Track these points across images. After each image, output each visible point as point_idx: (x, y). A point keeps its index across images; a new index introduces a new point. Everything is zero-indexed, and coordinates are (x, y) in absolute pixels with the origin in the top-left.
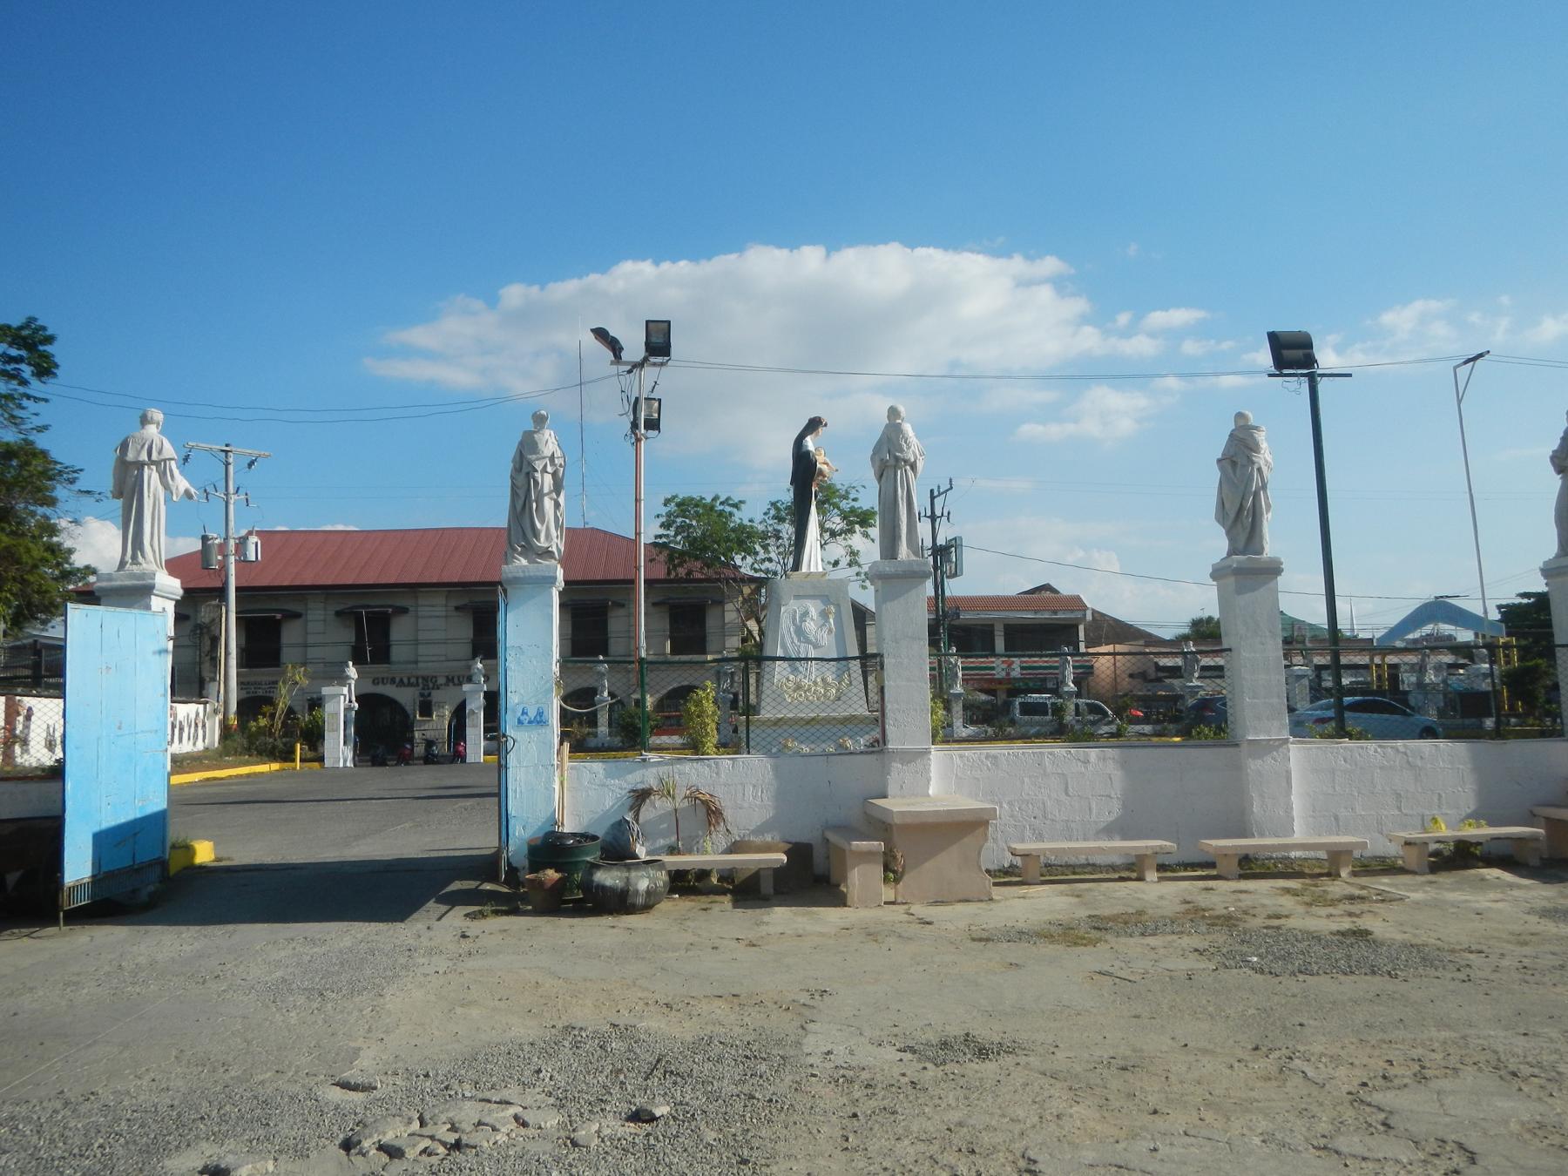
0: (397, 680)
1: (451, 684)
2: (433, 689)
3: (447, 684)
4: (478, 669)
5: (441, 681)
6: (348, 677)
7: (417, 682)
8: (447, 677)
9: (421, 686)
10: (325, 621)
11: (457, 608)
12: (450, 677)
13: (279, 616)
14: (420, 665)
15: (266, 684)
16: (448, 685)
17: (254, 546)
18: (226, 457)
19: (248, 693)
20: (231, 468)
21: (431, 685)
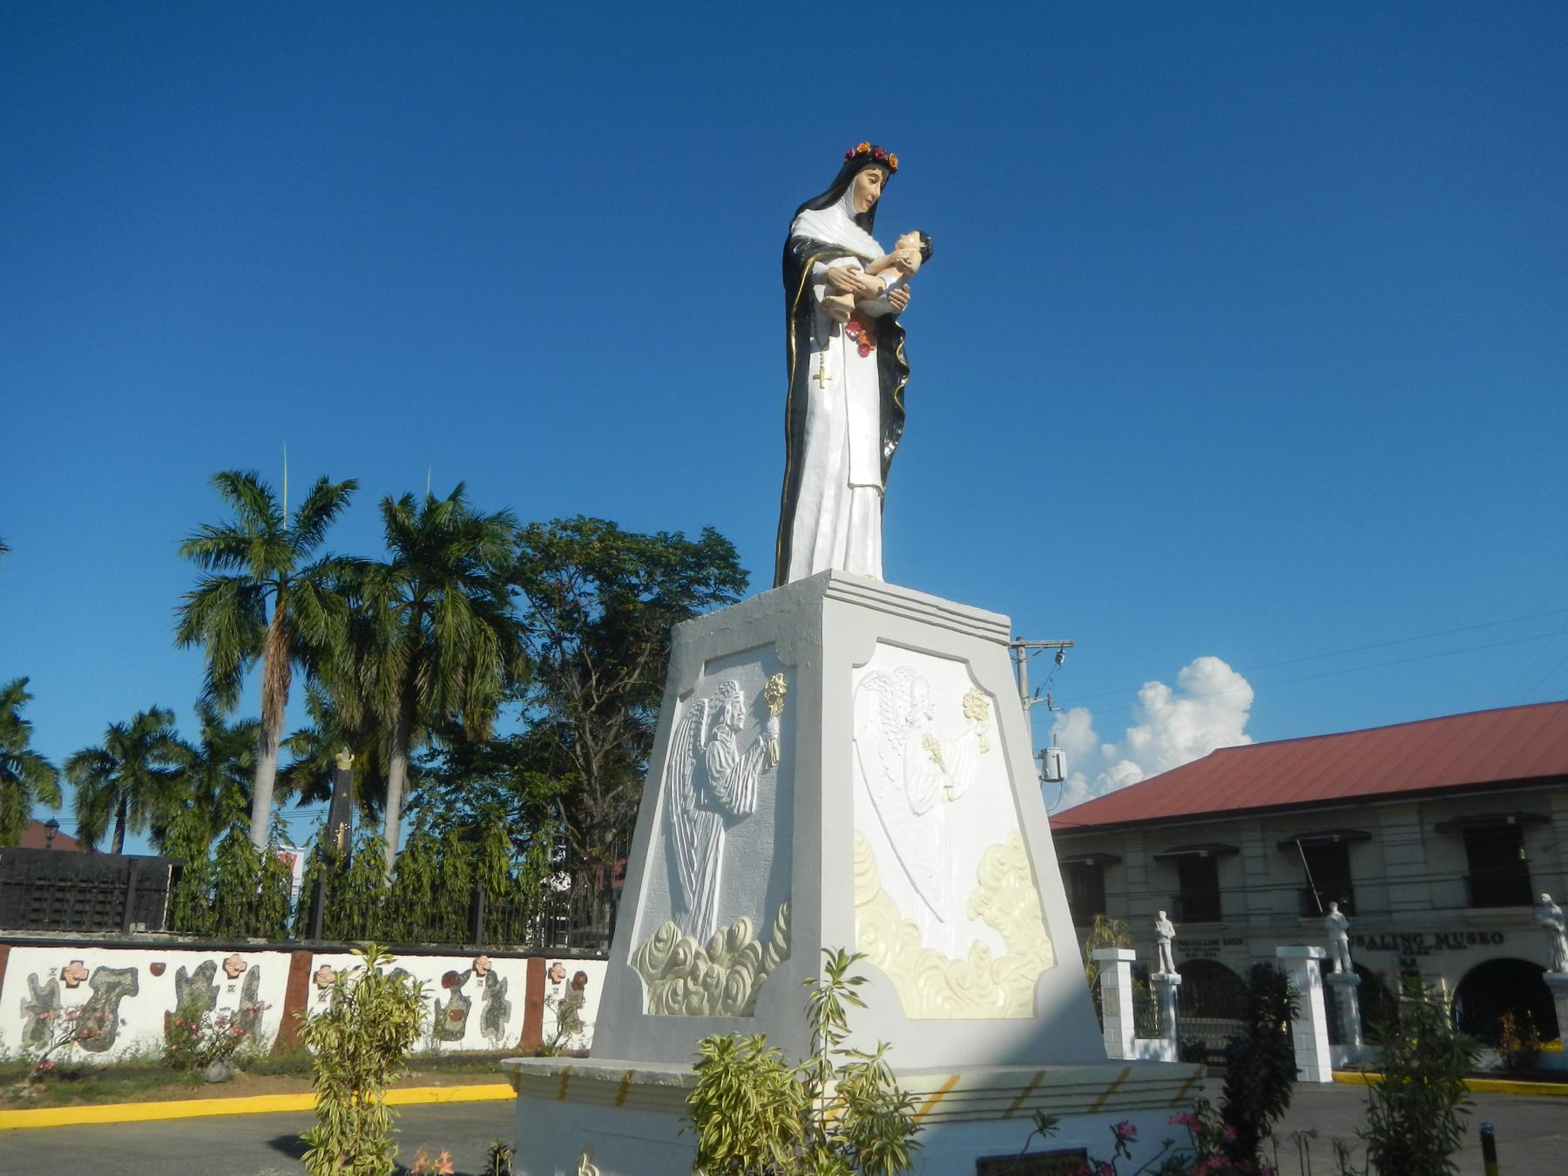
0: (1367, 939)
1: (1445, 947)
2: (1419, 953)
3: (1438, 947)
4: (1333, 920)
5: (1430, 941)
6: (1159, 935)
7: (1395, 944)
8: (1437, 936)
9: (1401, 949)
10: (1265, 856)
11: (1440, 828)
12: (1442, 936)
13: (1203, 853)
14: (1396, 916)
15: (1206, 944)
16: (1441, 948)
17: (1055, 759)
18: (1018, 655)
19: (1188, 955)
20: (1024, 665)
21: (1415, 948)
